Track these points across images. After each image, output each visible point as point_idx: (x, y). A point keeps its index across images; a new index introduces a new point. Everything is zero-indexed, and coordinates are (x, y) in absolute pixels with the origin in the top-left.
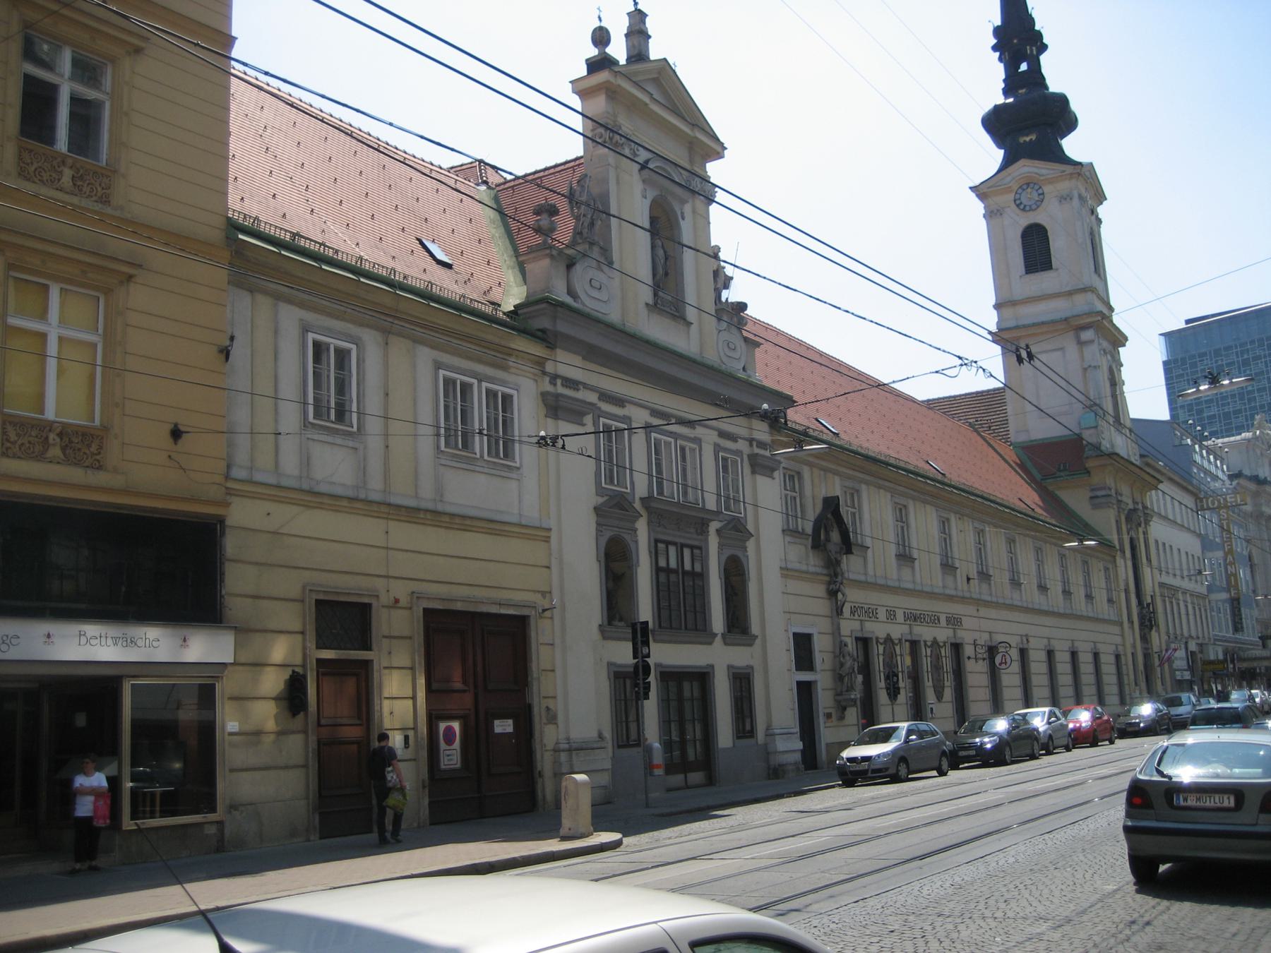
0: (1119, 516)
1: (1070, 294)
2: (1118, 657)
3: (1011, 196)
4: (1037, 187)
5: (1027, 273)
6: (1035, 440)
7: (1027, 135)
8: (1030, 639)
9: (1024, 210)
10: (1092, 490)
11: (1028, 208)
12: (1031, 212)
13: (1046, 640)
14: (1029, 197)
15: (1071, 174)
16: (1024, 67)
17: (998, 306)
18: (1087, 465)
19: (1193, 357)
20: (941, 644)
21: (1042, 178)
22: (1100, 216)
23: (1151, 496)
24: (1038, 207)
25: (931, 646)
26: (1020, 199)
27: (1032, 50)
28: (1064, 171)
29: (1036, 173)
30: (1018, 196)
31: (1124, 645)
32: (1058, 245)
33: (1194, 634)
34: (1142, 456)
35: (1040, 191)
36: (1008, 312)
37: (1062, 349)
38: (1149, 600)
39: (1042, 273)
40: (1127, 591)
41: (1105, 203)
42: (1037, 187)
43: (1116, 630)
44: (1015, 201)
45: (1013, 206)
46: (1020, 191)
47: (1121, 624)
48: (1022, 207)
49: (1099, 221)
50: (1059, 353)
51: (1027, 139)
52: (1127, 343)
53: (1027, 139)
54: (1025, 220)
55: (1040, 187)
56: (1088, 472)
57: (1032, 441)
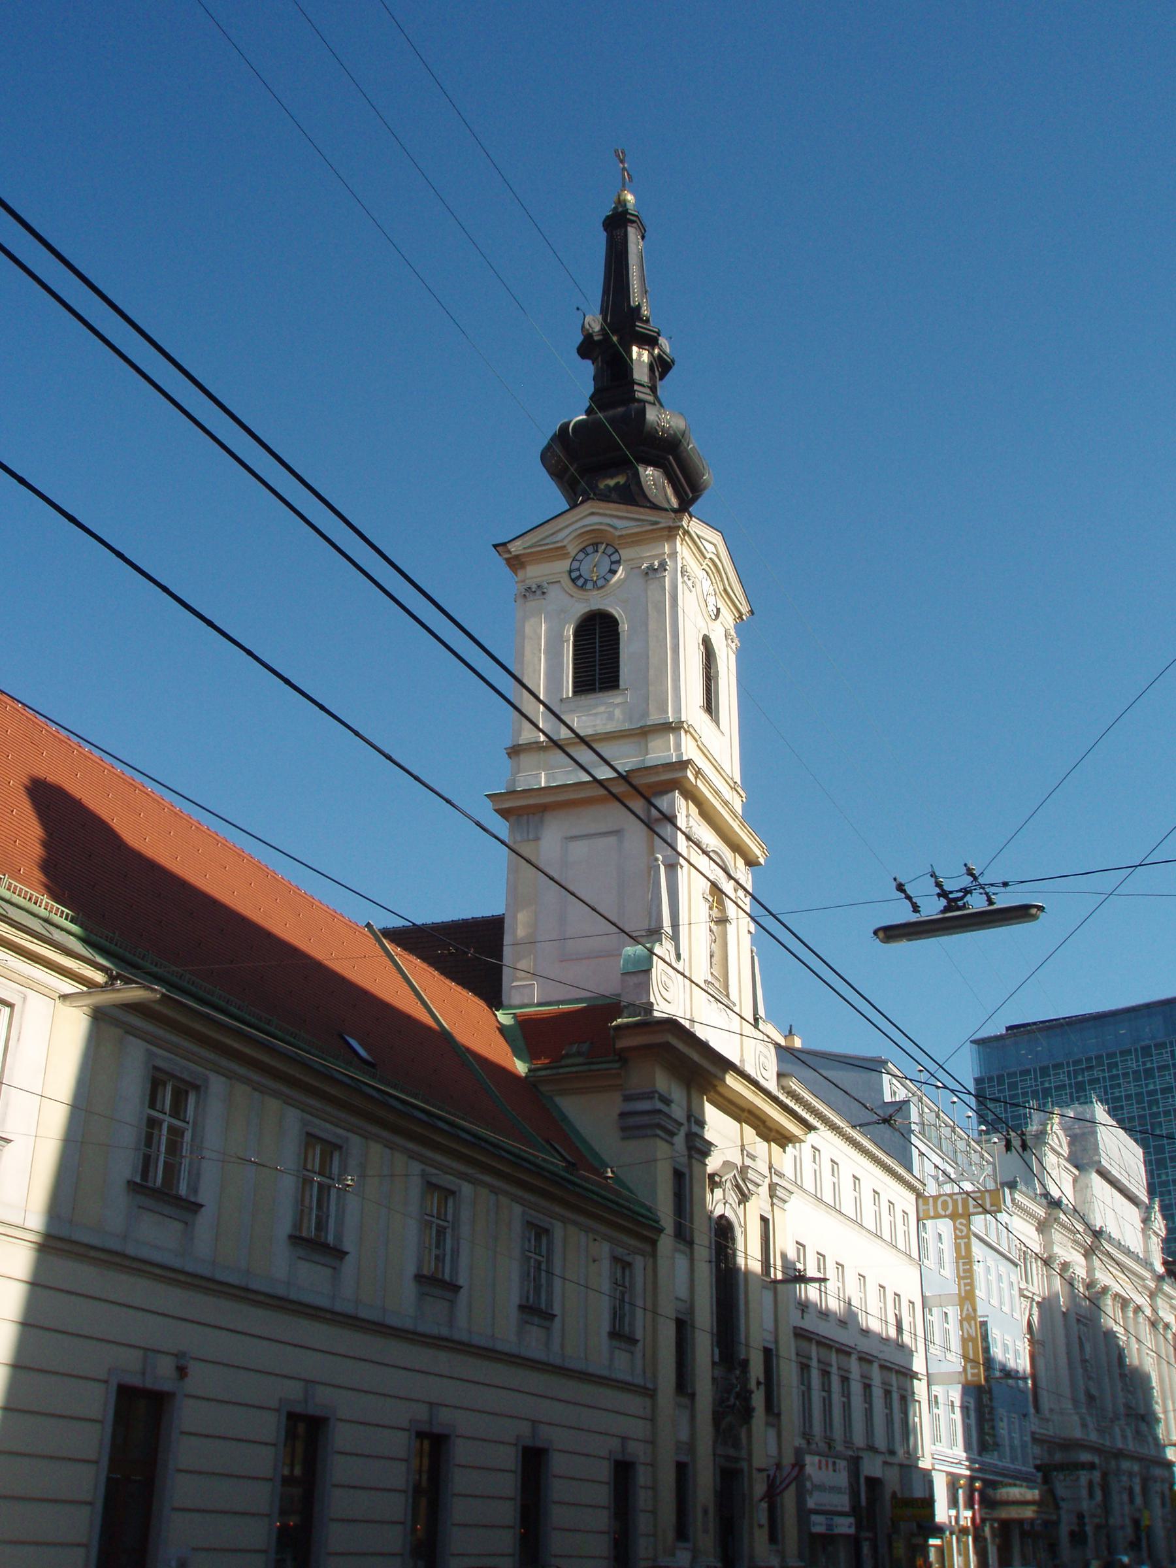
3: (565, 565)
4: (610, 550)
7: (612, 477)
10: (627, 1099)
14: (594, 564)
19: (1013, 1075)
21: (617, 533)
26: (578, 569)
28: (657, 523)
29: (609, 525)
30: (576, 565)
31: (652, 1442)
37: (617, 832)
39: (600, 695)
40: (683, 1326)
45: (566, 581)
47: (650, 1393)
48: (580, 582)
50: (612, 840)
51: (611, 483)
53: (611, 483)
54: (580, 607)
55: (617, 551)
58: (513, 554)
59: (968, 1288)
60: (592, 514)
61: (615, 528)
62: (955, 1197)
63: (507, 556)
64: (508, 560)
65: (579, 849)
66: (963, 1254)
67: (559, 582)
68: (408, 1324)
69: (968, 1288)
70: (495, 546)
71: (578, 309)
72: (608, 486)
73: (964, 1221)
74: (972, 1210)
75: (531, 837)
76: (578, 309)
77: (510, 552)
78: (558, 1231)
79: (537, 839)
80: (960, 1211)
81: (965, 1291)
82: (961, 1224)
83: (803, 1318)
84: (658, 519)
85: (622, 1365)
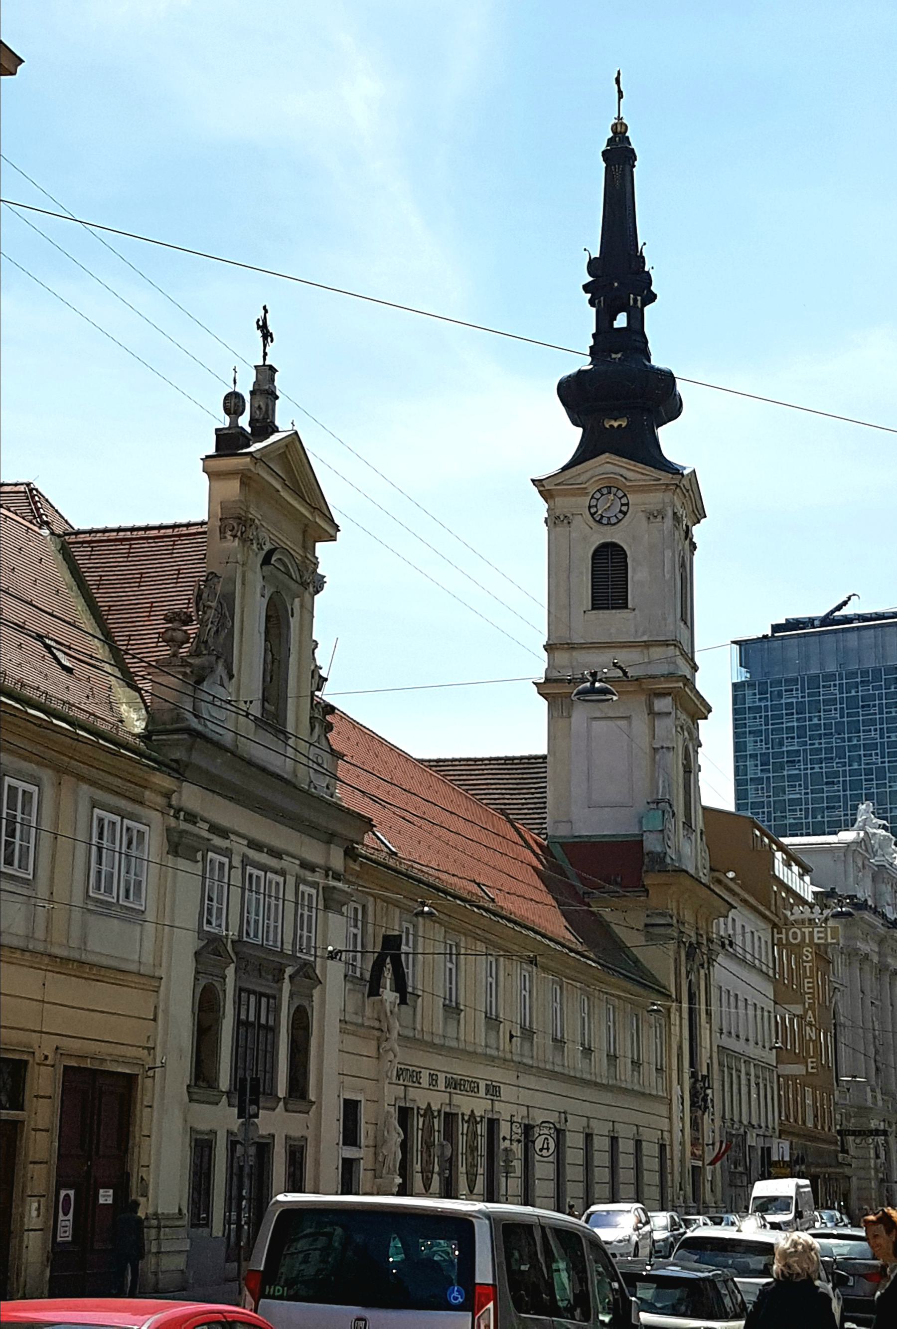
0: (679, 953)
1: (647, 645)
2: (662, 1147)
3: (586, 501)
4: (620, 494)
5: (593, 609)
7: (615, 420)
8: (569, 1117)
12: (609, 527)
13: (659, 1132)
14: (607, 505)
16: (621, 321)
17: (548, 648)
20: (478, 1119)
21: (628, 484)
22: (694, 540)
23: (718, 925)
25: (424, 1116)
27: (635, 301)
30: (594, 502)
31: (670, 1132)
33: (754, 1122)
34: (712, 869)
35: (624, 501)
37: (628, 718)
38: (705, 1073)
41: (703, 521)
42: (620, 494)
43: (663, 1110)
44: (590, 507)
46: (598, 495)
49: (693, 546)
51: (616, 424)
52: (710, 716)
53: (616, 424)
64: (540, 492)
70: (533, 481)
72: (611, 426)
77: (543, 486)
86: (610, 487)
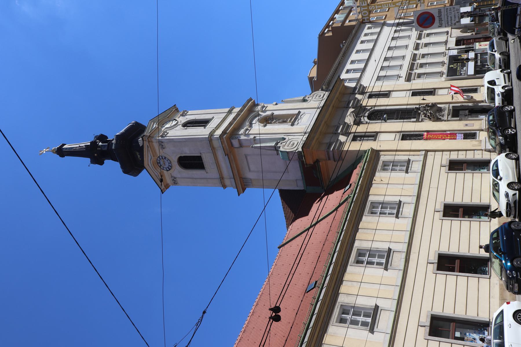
3: (165, 172)
6: (302, 176)
7: (138, 156)
9: (171, 167)
10: (329, 159)
11: (170, 165)
15: (149, 142)
18: (312, 163)
24: (168, 159)
30: (165, 169)
32: (188, 152)
36: (227, 182)
44: (167, 171)
50: (248, 158)
51: (139, 156)
53: (139, 156)
54: (177, 168)
56: (317, 161)
57: (303, 178)
58: (164, 187)
59: (392, 4)
60: (148, 165)
61: (151, 158)
62: (362, 10)
63: (165, 189)
65: (252, 167)
66: (381, 6)
67: (171, 174)
68: (401, 273)
69: (392, 4)
71: (89, 166)
72: (140, 157)
73: (370, 7)
74: (366, 4)
75: (250, 182)
76: (89, 166)
78: (366, 245)
79: (251, 179)
80: (367, 8)
81: (393, 5)
82: (371, 8)
83: (402, 77)
84: (147, 146)
85: (416, 167)
86: (157, 163)
